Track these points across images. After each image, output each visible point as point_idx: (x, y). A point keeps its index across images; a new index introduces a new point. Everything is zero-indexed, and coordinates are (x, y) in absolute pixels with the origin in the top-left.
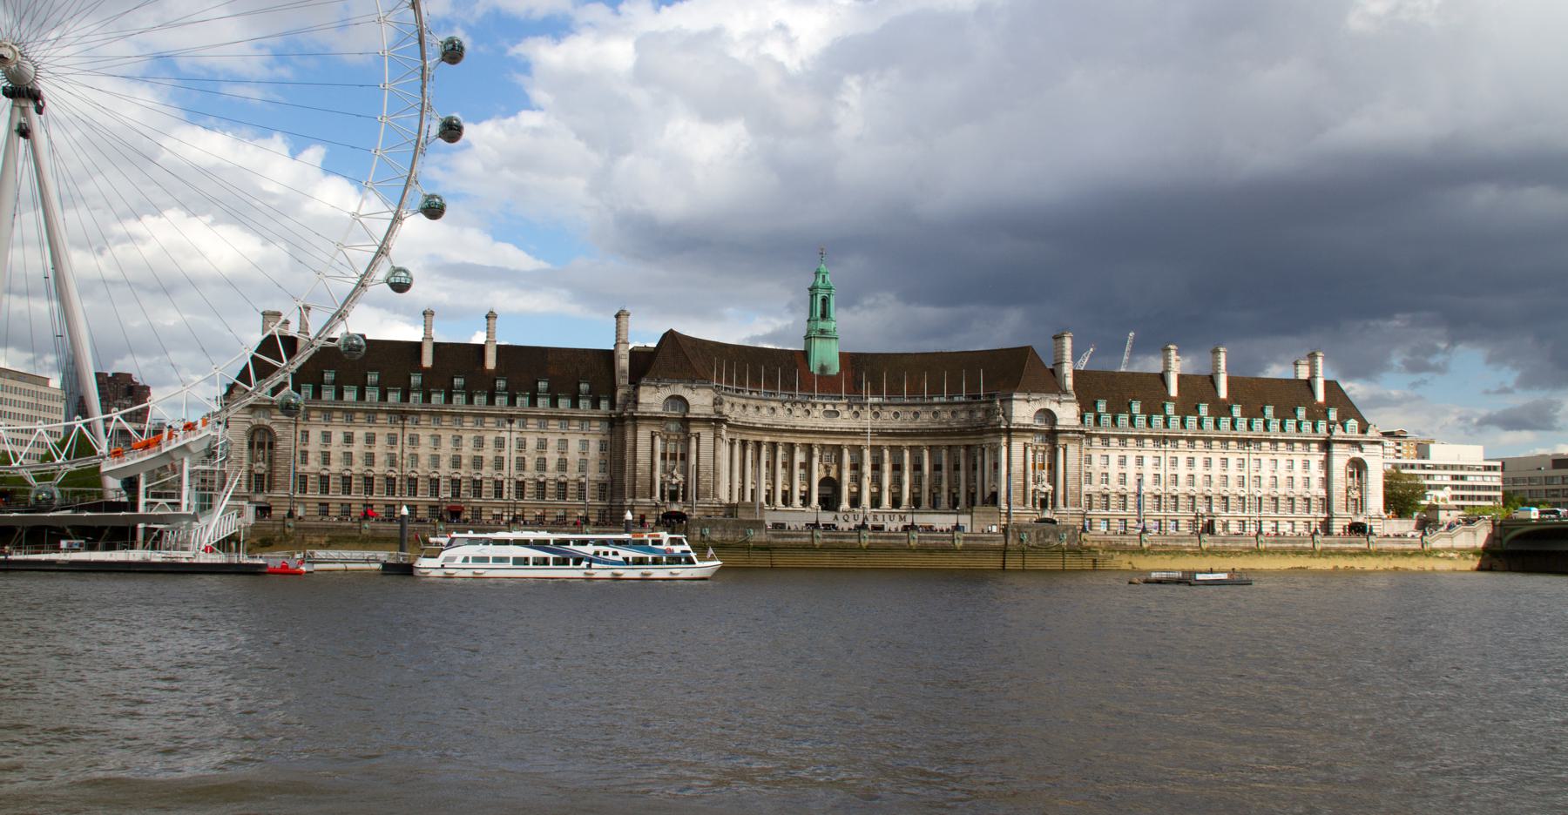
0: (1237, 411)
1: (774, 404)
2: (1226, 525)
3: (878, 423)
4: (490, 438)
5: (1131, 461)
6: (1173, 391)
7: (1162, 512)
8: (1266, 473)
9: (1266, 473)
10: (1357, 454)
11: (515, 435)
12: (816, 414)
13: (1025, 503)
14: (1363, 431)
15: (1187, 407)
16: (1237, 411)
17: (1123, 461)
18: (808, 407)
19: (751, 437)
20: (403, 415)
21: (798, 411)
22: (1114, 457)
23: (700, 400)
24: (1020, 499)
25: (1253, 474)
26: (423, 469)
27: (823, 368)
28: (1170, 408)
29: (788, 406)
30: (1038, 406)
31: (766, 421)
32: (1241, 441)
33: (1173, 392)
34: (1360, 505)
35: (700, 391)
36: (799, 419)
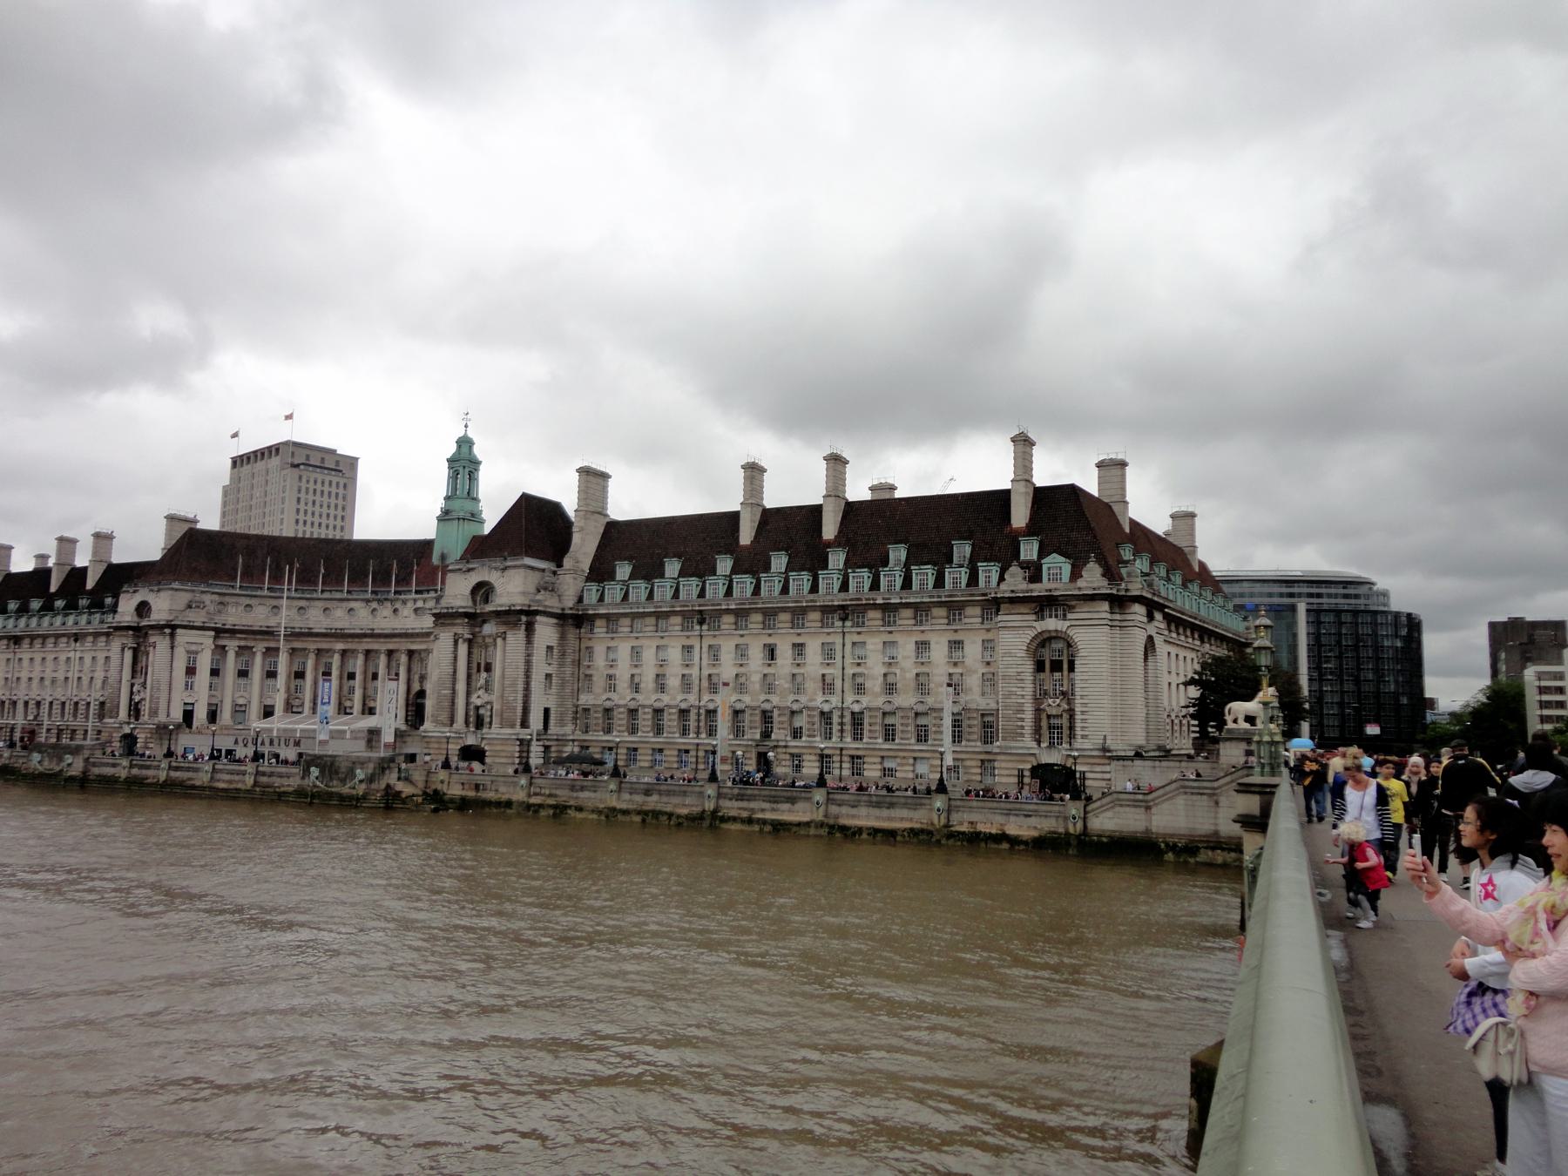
0: (837, 559)
1: (353, 604)
2: (797, 760)
3: (299, 624)
4: (63, 657)
5: (649, 656)
6: (746, 536)
7: (691, 739)
8: (875, 667)
9: (875, 667)
10: (1052, 624)
11: (78, 655)
12: (406, 612)
13: (452, 721)
14: (1075, 575)
15: (752, 563)
16: (837, 559)
17: (636, 653)
18: (398, 605)
19: (312, 645)
20: (16, 640)
21: (386, 610)
22: (624, 650)
23: (164, 604)
24: (444, 716)
25: (850, 671)
26: (21, 694)
27: (443, 557)
28: (724, 565)
29: (374, 605)
30: (474, 579)
31: (339, 625)
32: (827, 610)
33: (746, 536)
34: (1056, 725)
35: (162, 594)
36: (384, 619)
